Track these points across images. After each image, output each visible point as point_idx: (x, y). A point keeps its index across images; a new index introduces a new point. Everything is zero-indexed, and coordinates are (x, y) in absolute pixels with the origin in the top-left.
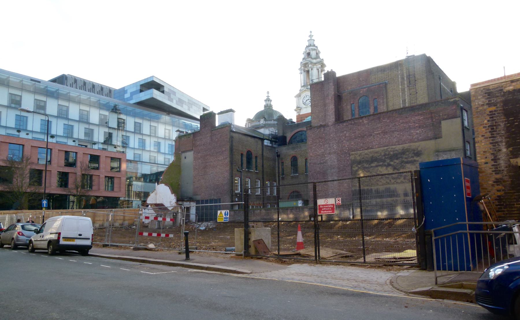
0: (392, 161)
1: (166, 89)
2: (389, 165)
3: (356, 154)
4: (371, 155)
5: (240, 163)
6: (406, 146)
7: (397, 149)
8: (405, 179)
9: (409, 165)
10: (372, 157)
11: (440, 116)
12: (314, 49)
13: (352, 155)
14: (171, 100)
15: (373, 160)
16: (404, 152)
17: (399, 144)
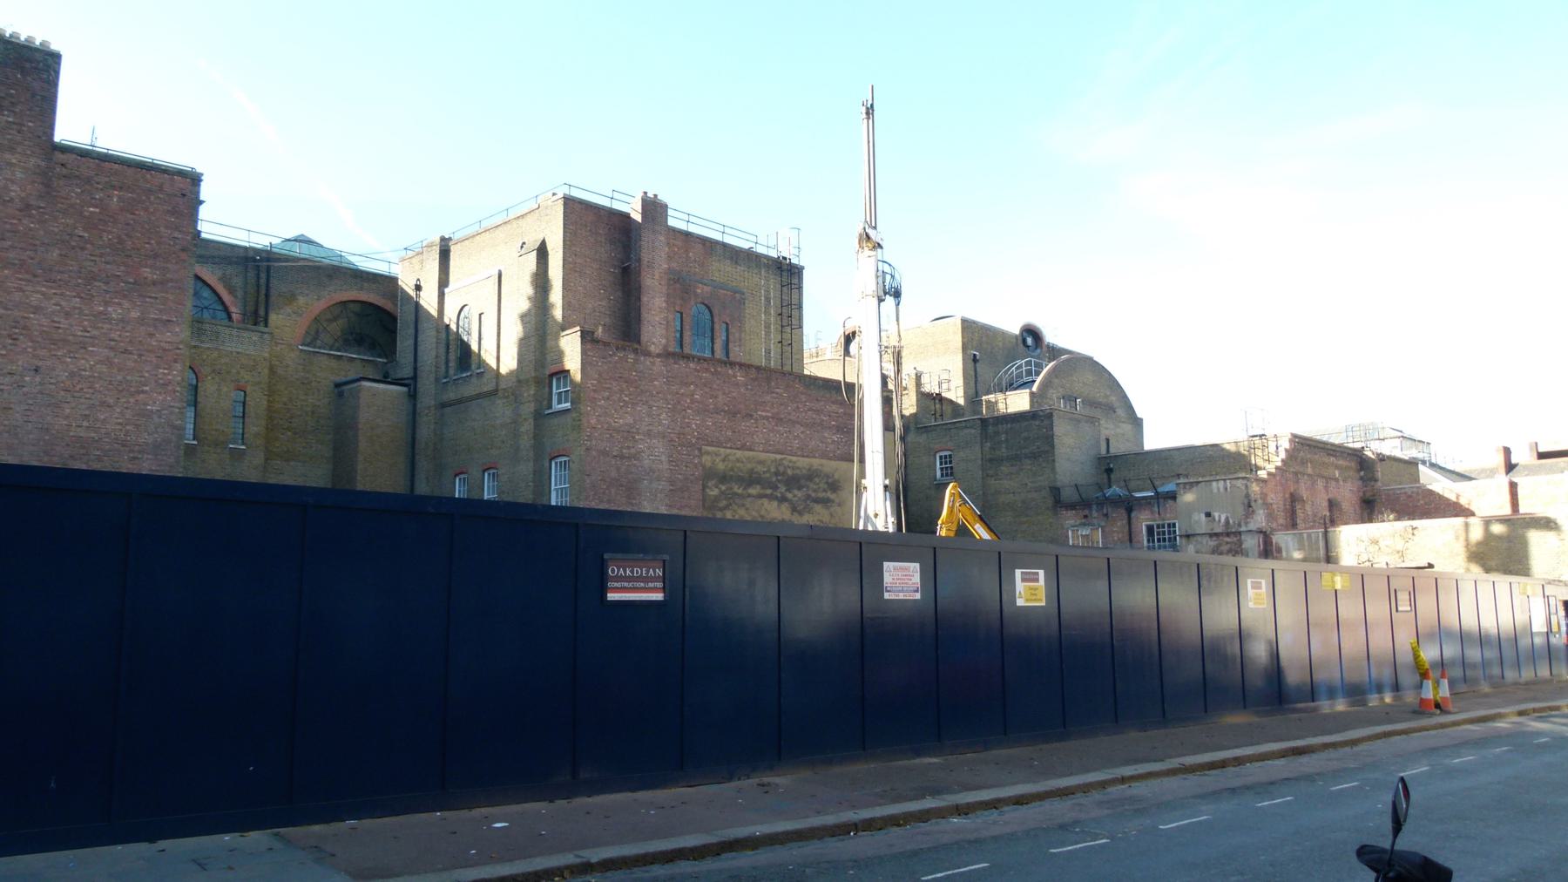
0: (788, 490)
2: (783, 499)
6: (816, 462)
7: (799, 464)
10: (752, 471)
13: (708, 453)
15: (751, 479)
16: (811, 475)
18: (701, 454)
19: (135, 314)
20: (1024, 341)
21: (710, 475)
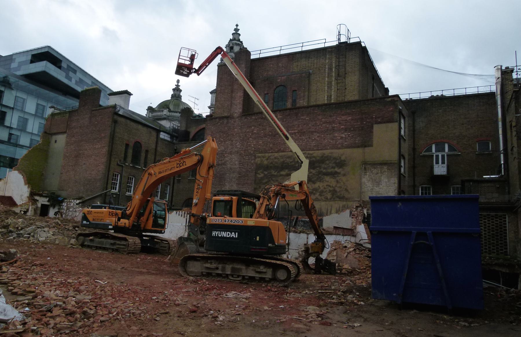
1: (64, 65)
3: (264, 157)
4: (282, 160)
5: (123, 155)
6: (327, 152)
7: (315, 155)
8: (320, 195)
9: (329, 177)
11: (372, 118)
12: (238, 45)
13: (259, 157)
14: (70, 79)
17: (318, 150)
18: (255, 157)
19: (100, 146)
21: (259, 167)
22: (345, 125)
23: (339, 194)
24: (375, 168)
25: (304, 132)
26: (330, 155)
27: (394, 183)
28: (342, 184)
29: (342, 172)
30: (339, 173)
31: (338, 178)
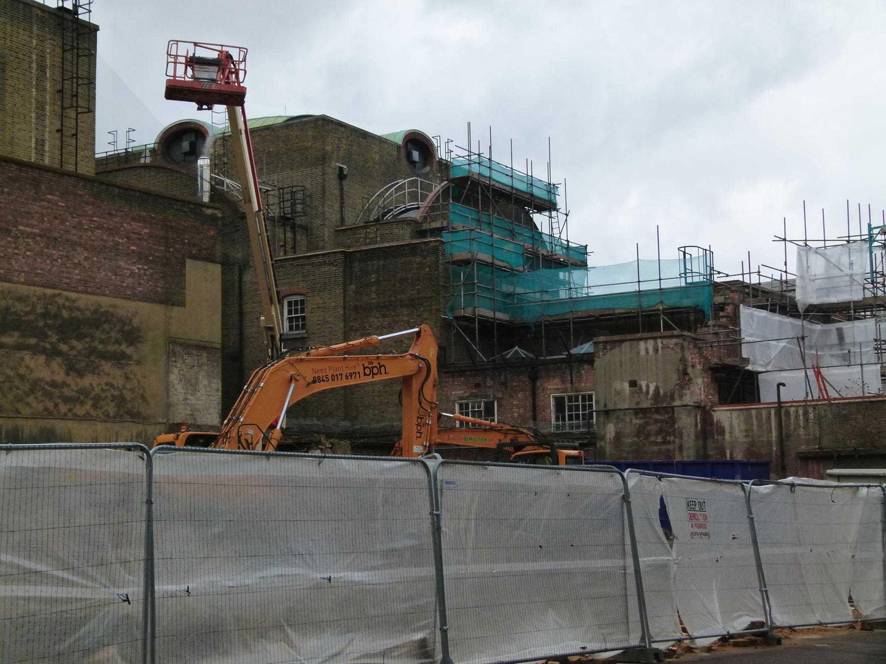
2: (54, 353)
6: (105, 302)
7: (81, 304)
8: (95, 406)
9: (110, 364)
10: (8, 308)
11: (184, 244)
16: (100, 319)
17: (86, 292)
20: (409, 156)
22: (138, 246)
23: (129, 406)
24: (189, 354)
25: (55, 239)
26: (111, 310)
27: (217, 390)
28: (135, 382)
29: (135, 357)
30: (130, 358)
31: (128, 369)
